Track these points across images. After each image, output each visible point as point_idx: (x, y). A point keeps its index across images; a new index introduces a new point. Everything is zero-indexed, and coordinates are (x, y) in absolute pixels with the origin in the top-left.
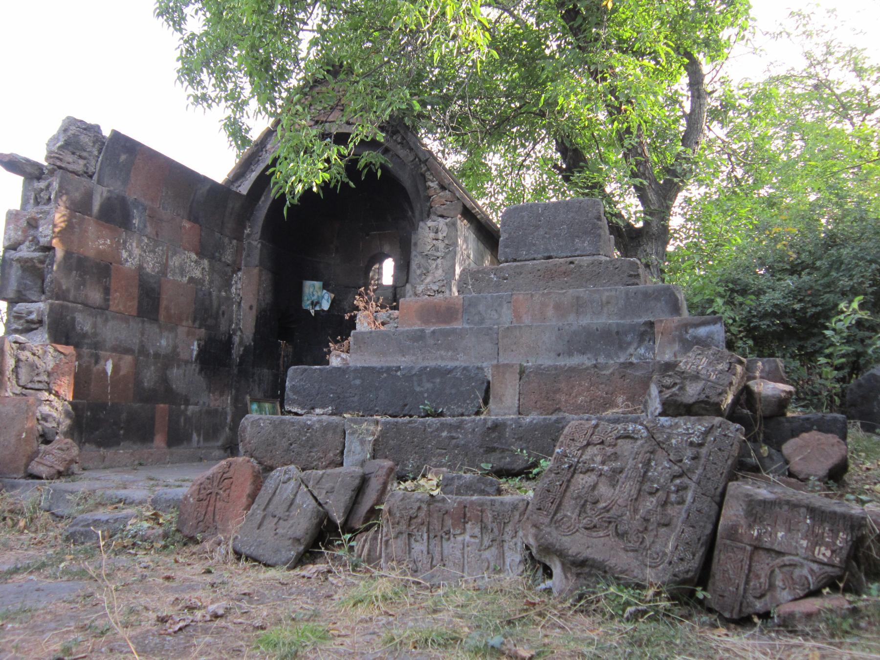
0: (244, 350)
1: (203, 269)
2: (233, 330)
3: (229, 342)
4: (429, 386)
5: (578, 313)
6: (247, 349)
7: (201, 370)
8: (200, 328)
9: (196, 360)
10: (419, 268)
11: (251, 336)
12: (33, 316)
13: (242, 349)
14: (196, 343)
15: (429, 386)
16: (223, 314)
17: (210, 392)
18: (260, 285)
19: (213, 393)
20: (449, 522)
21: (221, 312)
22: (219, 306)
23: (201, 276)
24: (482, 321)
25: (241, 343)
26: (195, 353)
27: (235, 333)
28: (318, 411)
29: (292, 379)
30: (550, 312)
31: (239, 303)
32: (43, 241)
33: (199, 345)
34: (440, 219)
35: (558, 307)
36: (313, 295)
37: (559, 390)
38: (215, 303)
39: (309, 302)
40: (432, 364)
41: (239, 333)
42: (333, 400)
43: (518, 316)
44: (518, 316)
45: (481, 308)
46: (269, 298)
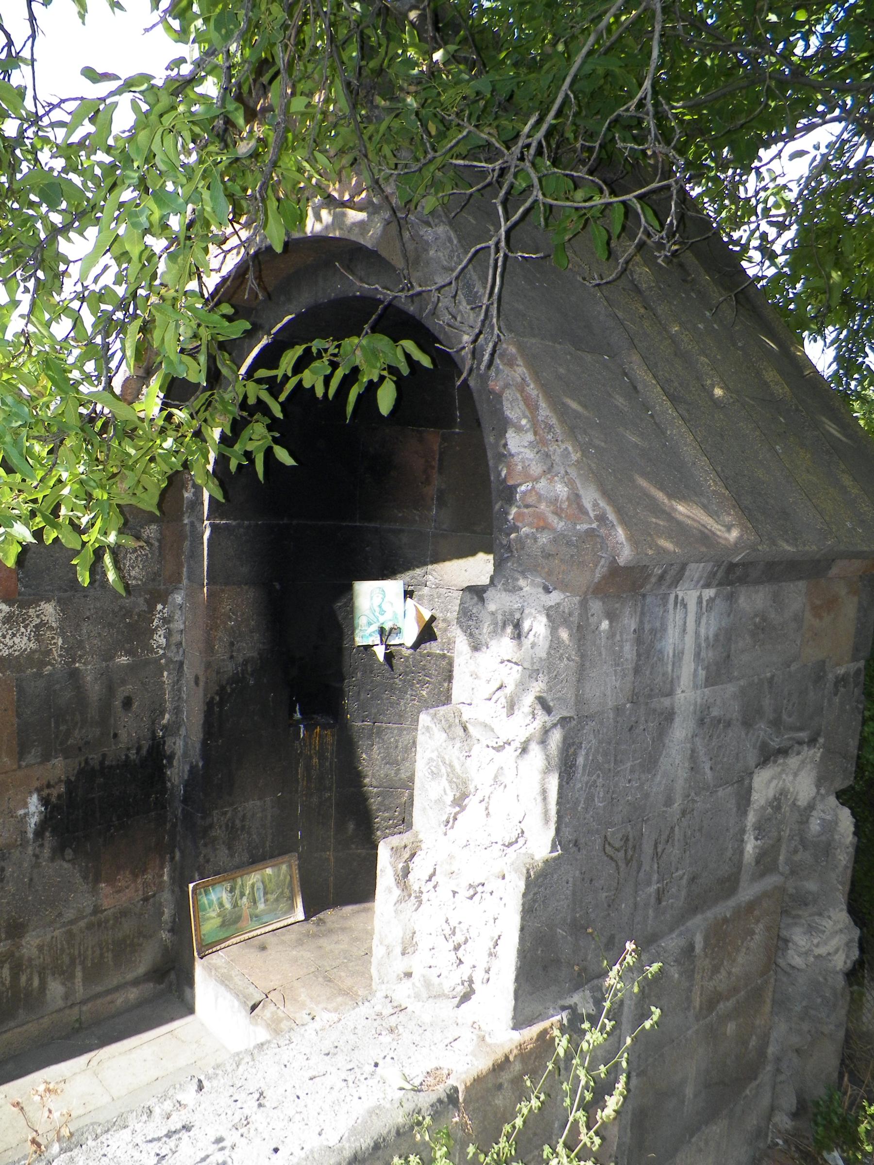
0: (191, 772)
1: (42, 624)
2: (165, 728)
3: (155, 757)
6: (193, 769)
7: (58, 852)
8: (46, 758)
9: (39, 833)
10: (435, 775)
11: (198, 746)
13: (187, 768)
14: (34, 800)
16: (127, 703)
17: (97, 880)
18: (211, 628)
19: (111, 881)
21: (118, 703)
22: (111, 690)
23: (32, 645)
25: (185, 754)
26: (33, 821)
27: (171, 729)
31: (181, 664)
33: (45, 801)
36: (383, 612)
38: (94, 689)
39: (375, 627)
41: (183, 731)
46: (250, 648)
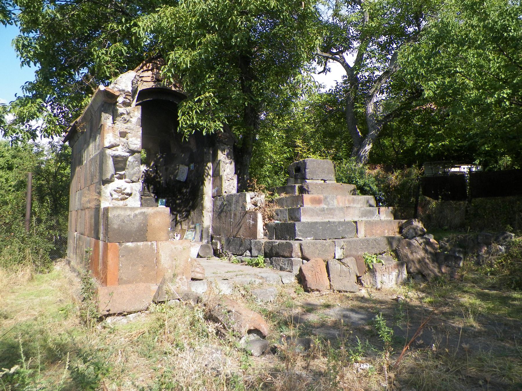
4: (341, 228)
5: (353, 203)
12: (128, 191)
15: (341, 228)
20: (391, 270)
24: (329, 204)
28: (309, 238)
29: (299, 227)
30: (347, 202)
32: (133, 147)
34: (225, 146)
35: (349, 201)
37: (373, 229)
40: (327, 220)
42: (313, 234)
43: (338, 203)
44: (338, 203)
45: (328, 199)
